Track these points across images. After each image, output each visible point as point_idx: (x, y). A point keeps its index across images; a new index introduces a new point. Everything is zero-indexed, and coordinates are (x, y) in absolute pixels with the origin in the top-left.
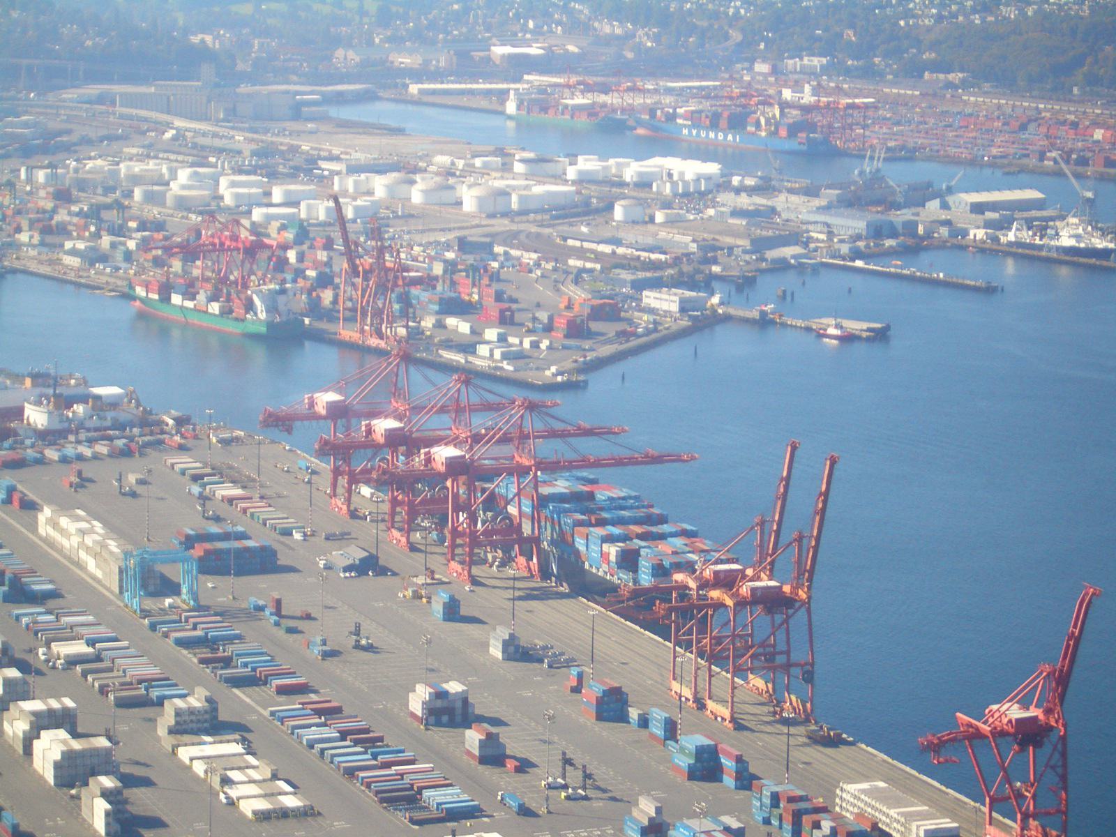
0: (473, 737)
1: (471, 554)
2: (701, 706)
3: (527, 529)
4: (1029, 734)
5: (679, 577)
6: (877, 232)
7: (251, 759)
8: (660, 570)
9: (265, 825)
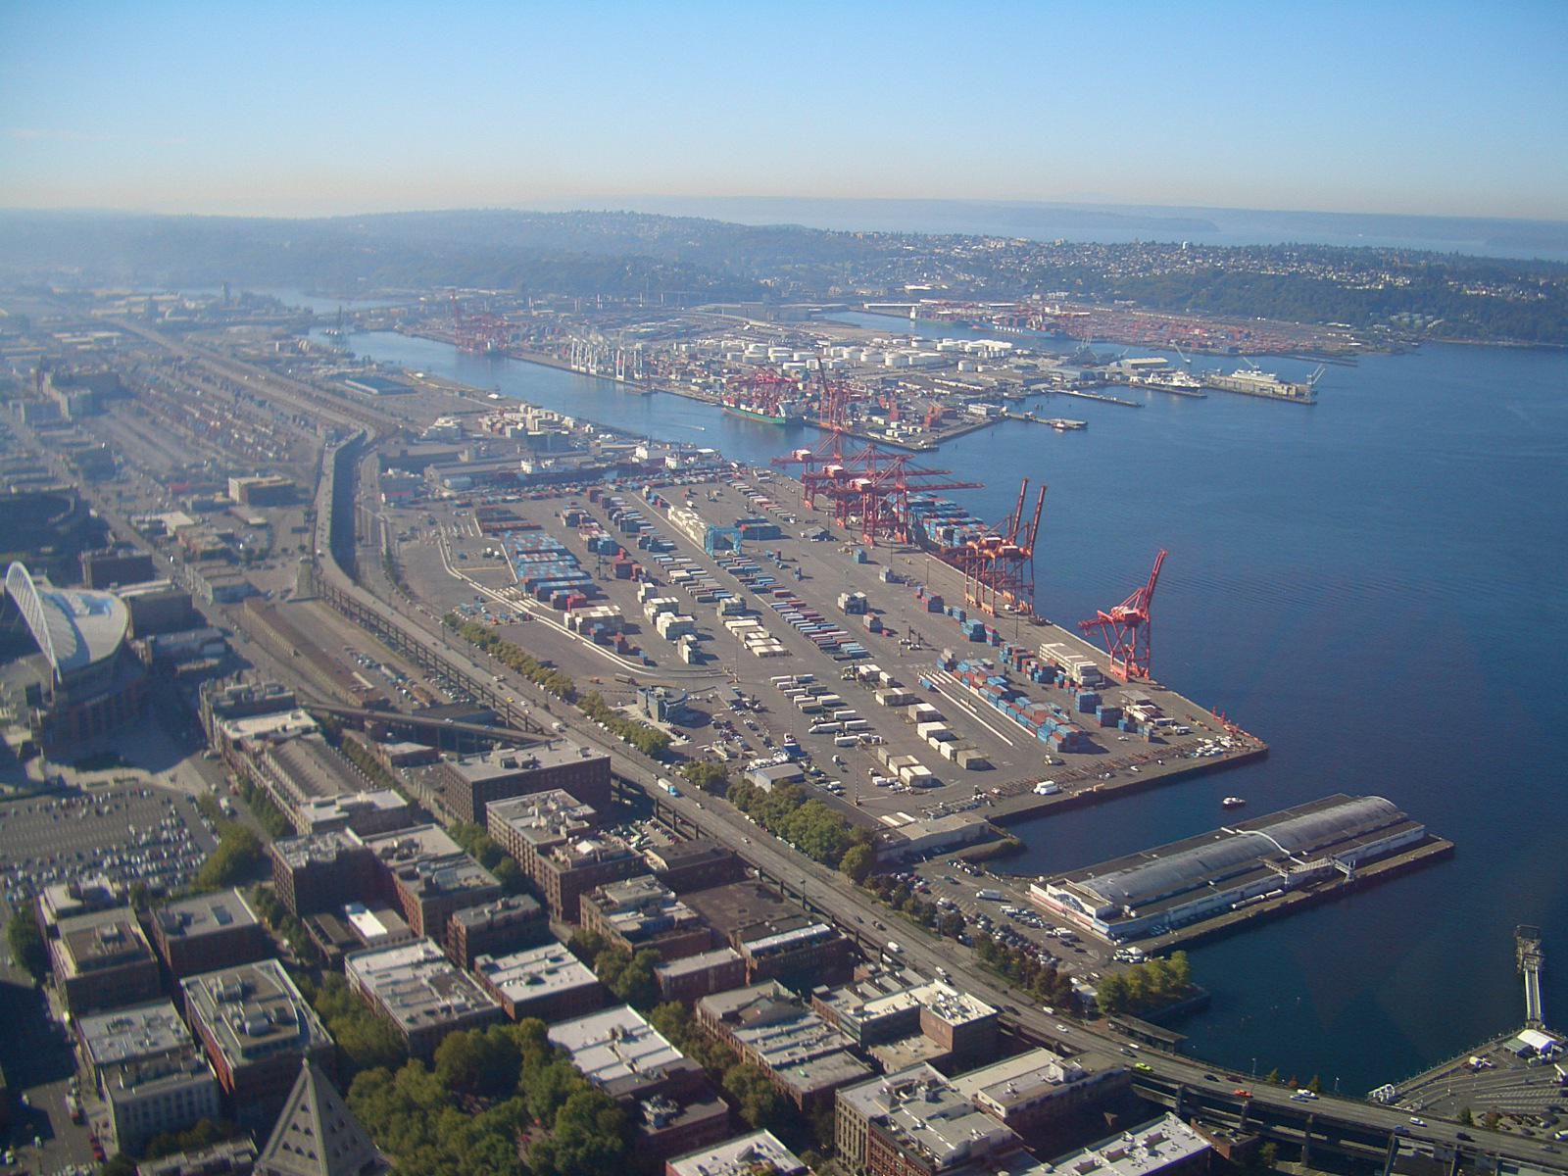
0: (867, 619)
1: (874, 531)
2: (980, 606)
3: (901, 519)
4: (1132, 621)
5: (969, 543)
6: (1086, 377)
7: (760, 628)
8: (963, 540)
9: (765, 659)
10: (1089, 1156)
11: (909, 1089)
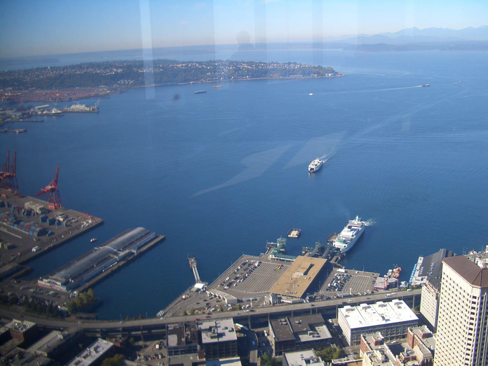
4: (52, 190)
6: (23, 114)
10: (77, 359)
11: (12, 357)
